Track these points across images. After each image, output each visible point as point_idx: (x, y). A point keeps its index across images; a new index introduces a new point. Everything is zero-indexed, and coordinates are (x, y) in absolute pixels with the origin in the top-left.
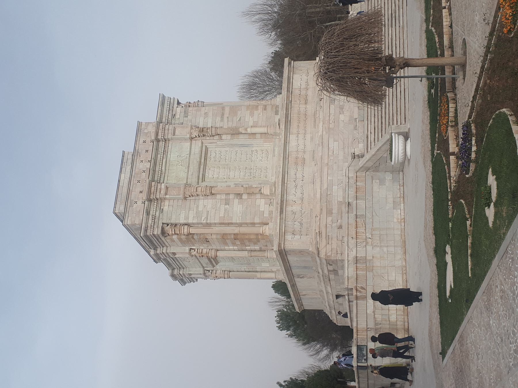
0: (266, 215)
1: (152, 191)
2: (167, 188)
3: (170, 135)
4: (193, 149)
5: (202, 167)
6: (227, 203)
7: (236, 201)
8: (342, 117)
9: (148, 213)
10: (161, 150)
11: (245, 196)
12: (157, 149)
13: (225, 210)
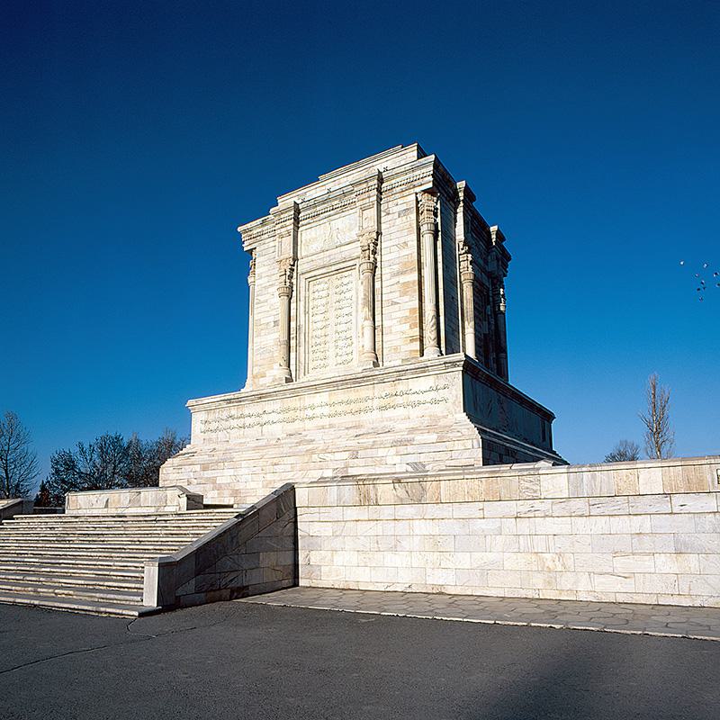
3: (361, 203)
5: (324, 271)
10: (346, 200)
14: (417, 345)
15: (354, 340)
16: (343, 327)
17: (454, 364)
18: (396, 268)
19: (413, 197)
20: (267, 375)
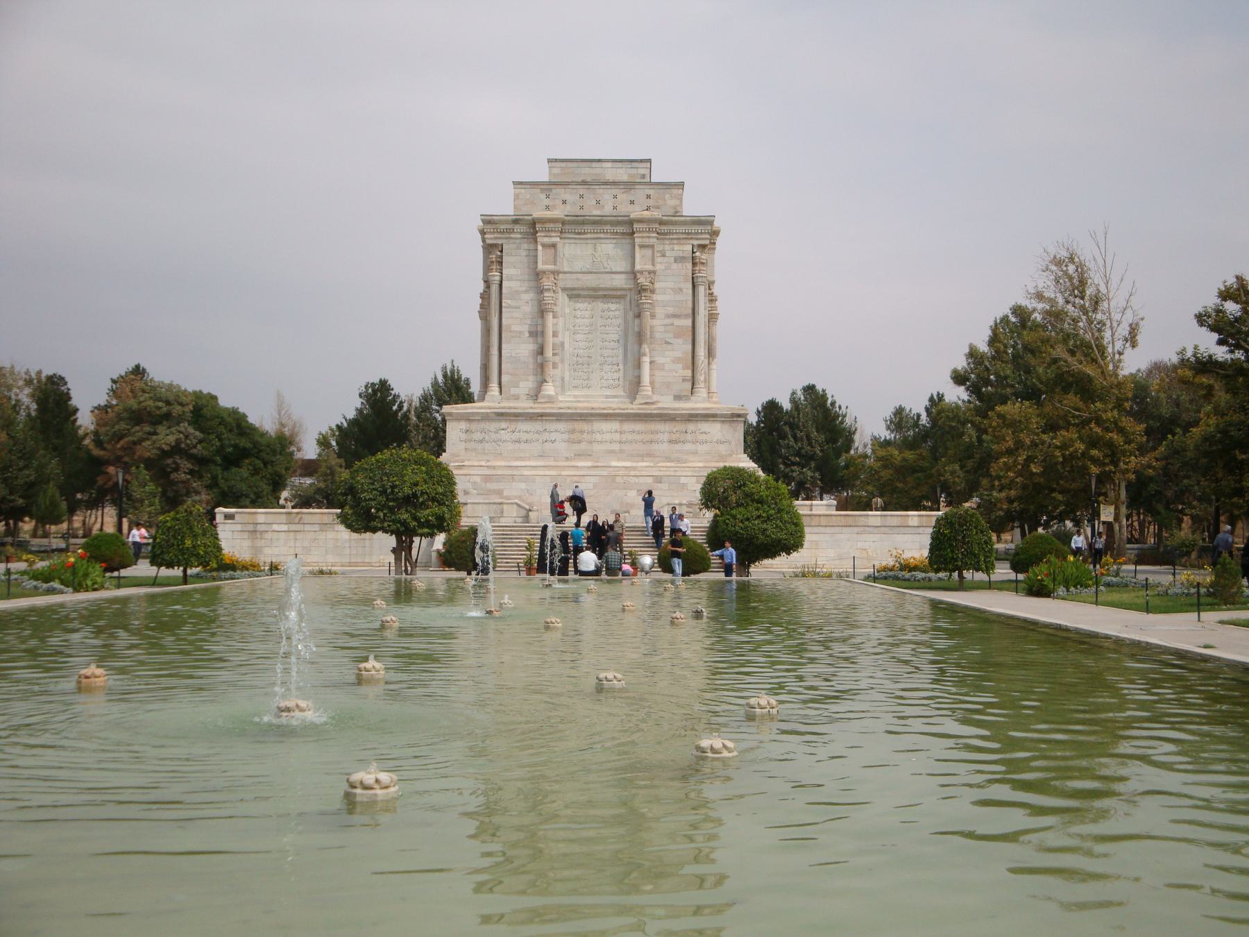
0: (513, 391)
1: (547, 225)
2: (554, 246)
11: (539, 357)
14: (689, 385)
16: (609, 352)
18: (671, 310)
20: (522, 384)
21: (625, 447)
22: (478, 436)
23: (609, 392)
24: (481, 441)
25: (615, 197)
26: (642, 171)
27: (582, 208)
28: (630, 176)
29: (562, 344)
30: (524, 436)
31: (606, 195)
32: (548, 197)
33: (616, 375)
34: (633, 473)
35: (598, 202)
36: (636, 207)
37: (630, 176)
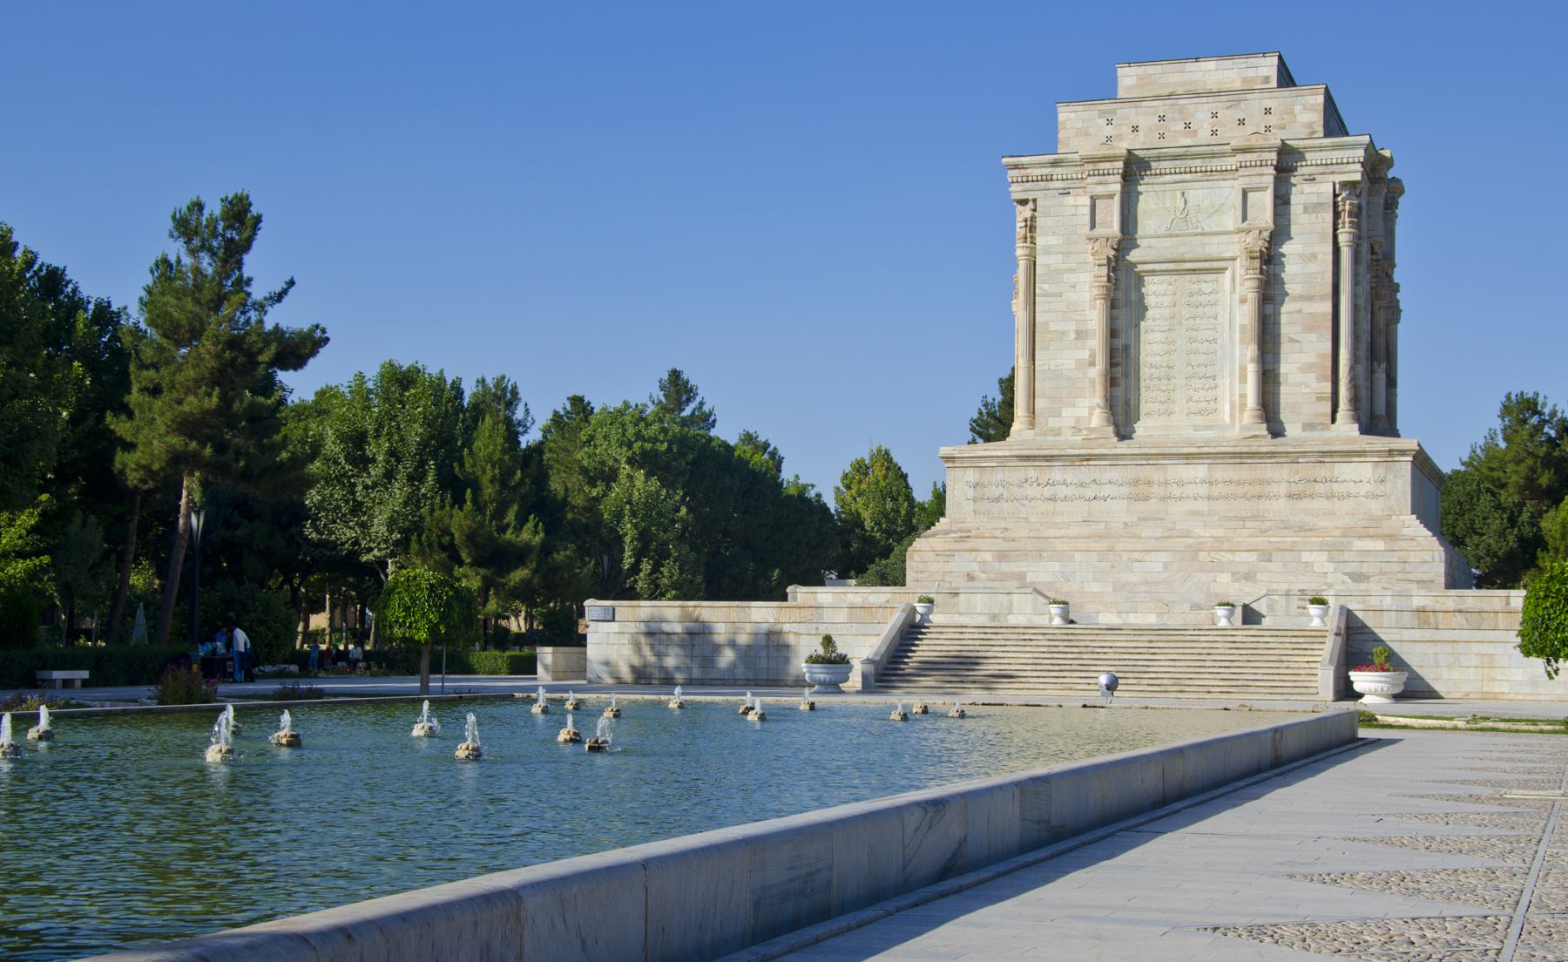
0: (1053, 423)
1: (1101, 166)
2: (1111, 196)
4: (1216, 239)
6: (1081, 335)
7: (1086, 355)
8: (1224, 578)
9: (1055, 164)
10: (1215, 164)
12: (1213, 155)
13: (1063, 333)
15: (1219, 381)
16: (1202, 359)
17: (1403, 452)
19: (1327, 189)
21: (1220, 506)
22: (994, 492)
23: (1199, 420)
24: (998, 500)
25: (1214, 115)
26: (1264, 72)
27: (1162, 136)
28: (1245, 80)
29: (1126, 348)
30: (1061, 491)
31: (1201, 114)
32: (1110, 122)
33: (1210, 394)
34: (1226, 546)
35: (1187, 126)
36: (1249, 129)
37: (1245, 80)
